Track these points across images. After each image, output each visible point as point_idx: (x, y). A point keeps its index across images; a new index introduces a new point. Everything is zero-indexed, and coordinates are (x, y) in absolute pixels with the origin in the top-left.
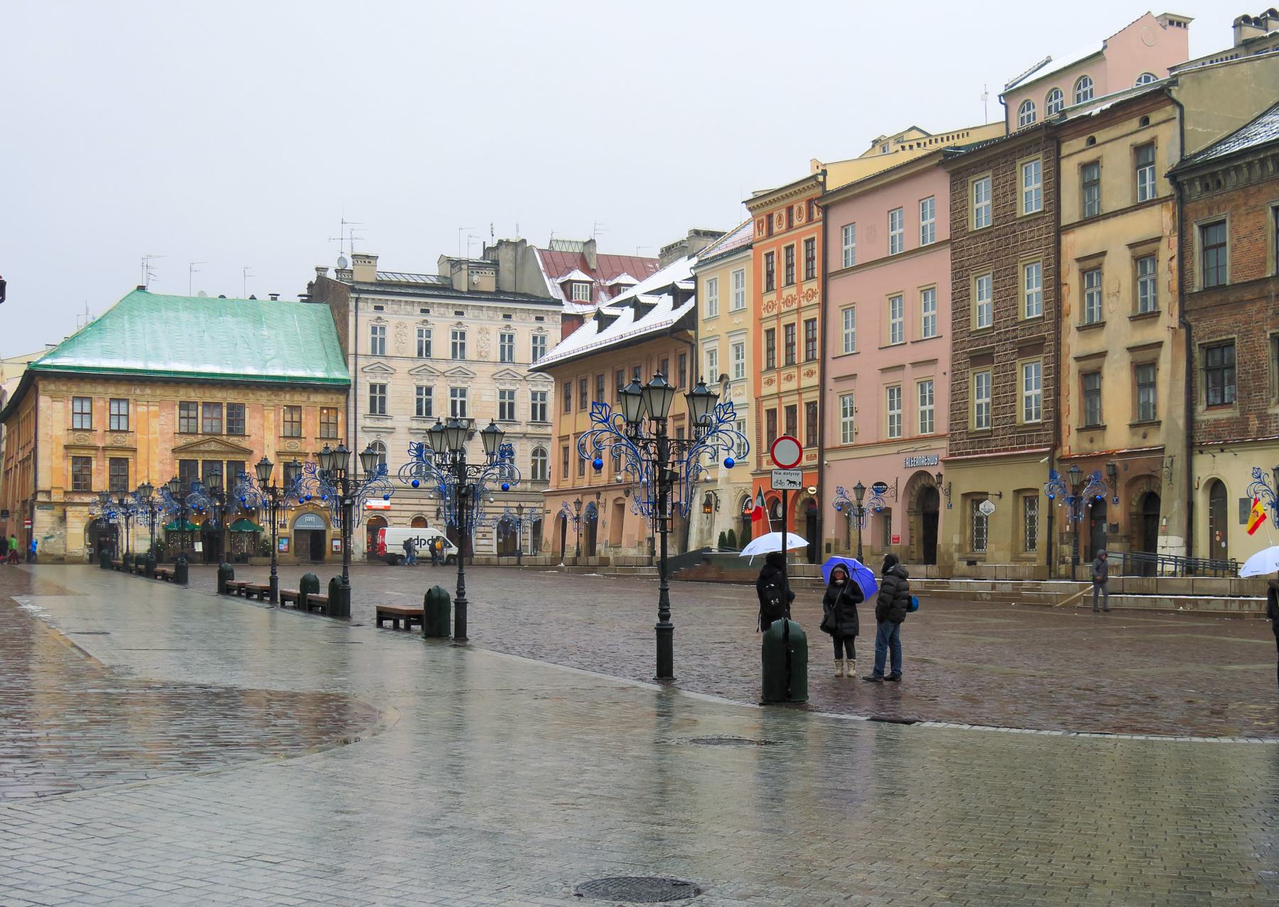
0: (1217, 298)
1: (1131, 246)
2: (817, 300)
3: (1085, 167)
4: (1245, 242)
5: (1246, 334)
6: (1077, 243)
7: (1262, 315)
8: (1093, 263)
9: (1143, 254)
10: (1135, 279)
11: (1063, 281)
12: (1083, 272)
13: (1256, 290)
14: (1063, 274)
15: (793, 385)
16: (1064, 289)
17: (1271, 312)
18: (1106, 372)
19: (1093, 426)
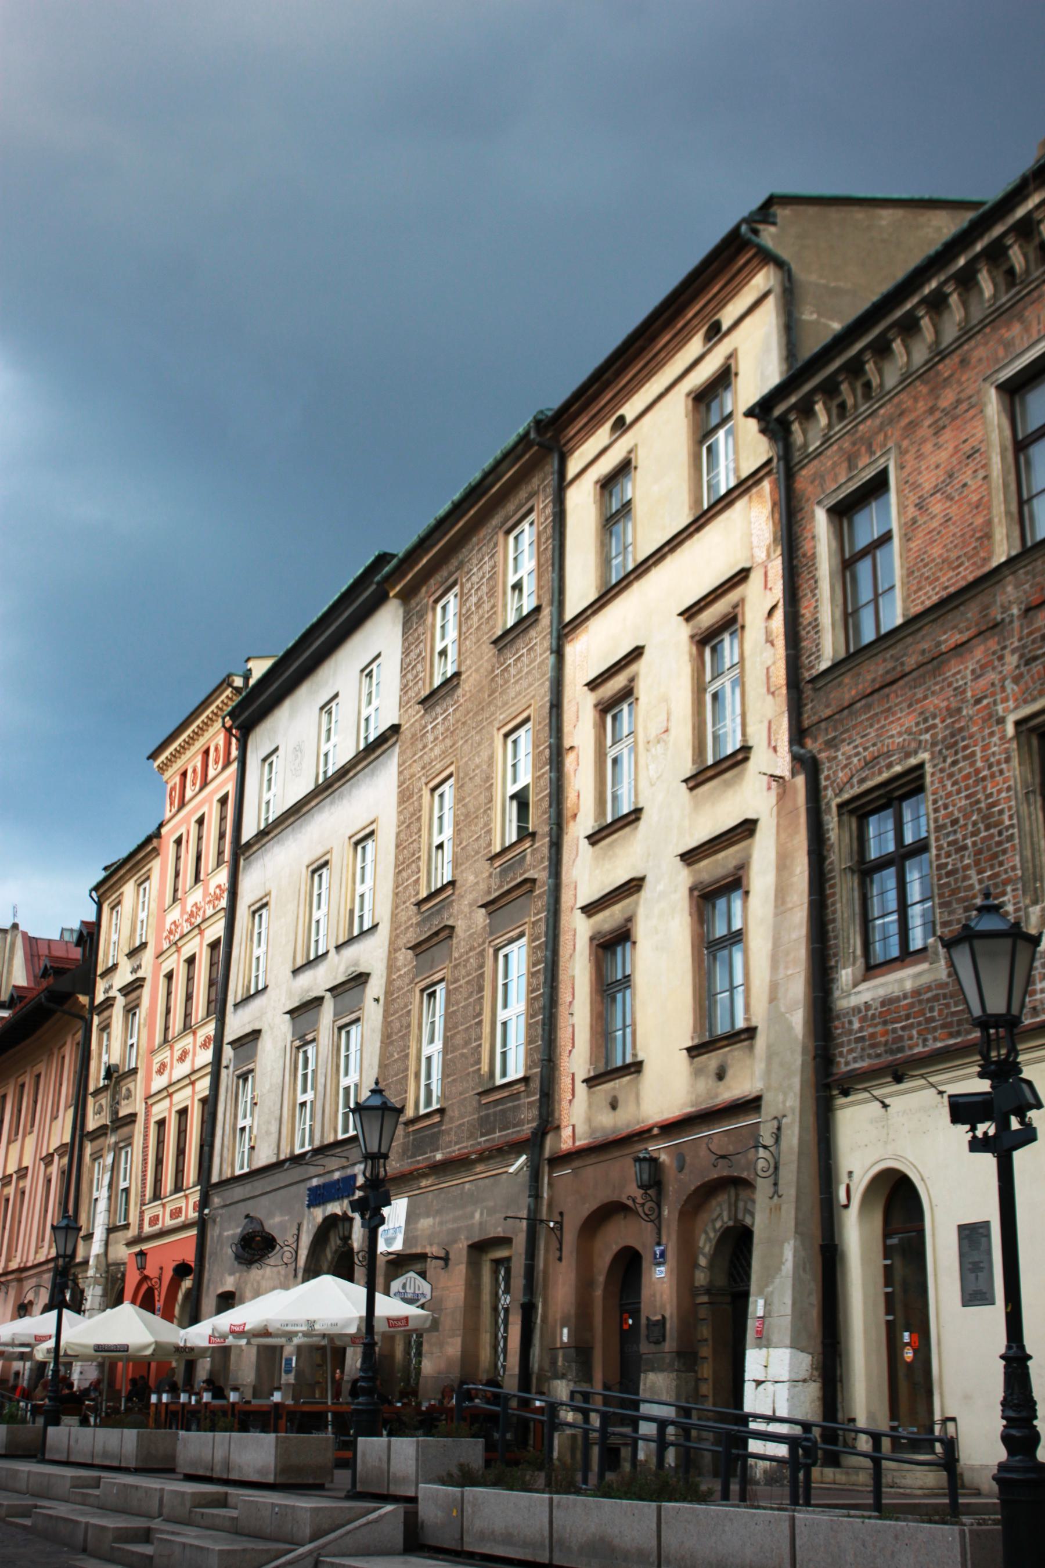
0: (874, 670)
1: (689, 614)
2: (223, 903)
3: (608, 484)
4: (937, 507)
5: (953, 743)
6: (590, 652)
7: (992, 676)
8: (618, 683)
9: (712, 626)
10: (699, 688)
11: (567, 743)
12: (607, 708)
13: (971, 612)
14: (567, 728)
15: (181, 1070)
16: (569, 760)
17: (1012, 660)
18: (642, 931)
19: (616, 1070)
